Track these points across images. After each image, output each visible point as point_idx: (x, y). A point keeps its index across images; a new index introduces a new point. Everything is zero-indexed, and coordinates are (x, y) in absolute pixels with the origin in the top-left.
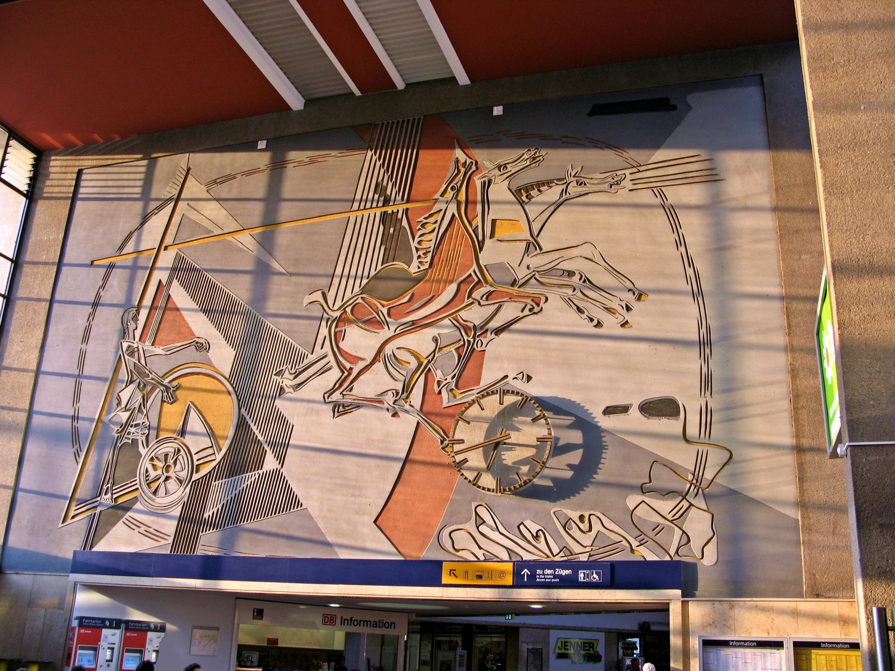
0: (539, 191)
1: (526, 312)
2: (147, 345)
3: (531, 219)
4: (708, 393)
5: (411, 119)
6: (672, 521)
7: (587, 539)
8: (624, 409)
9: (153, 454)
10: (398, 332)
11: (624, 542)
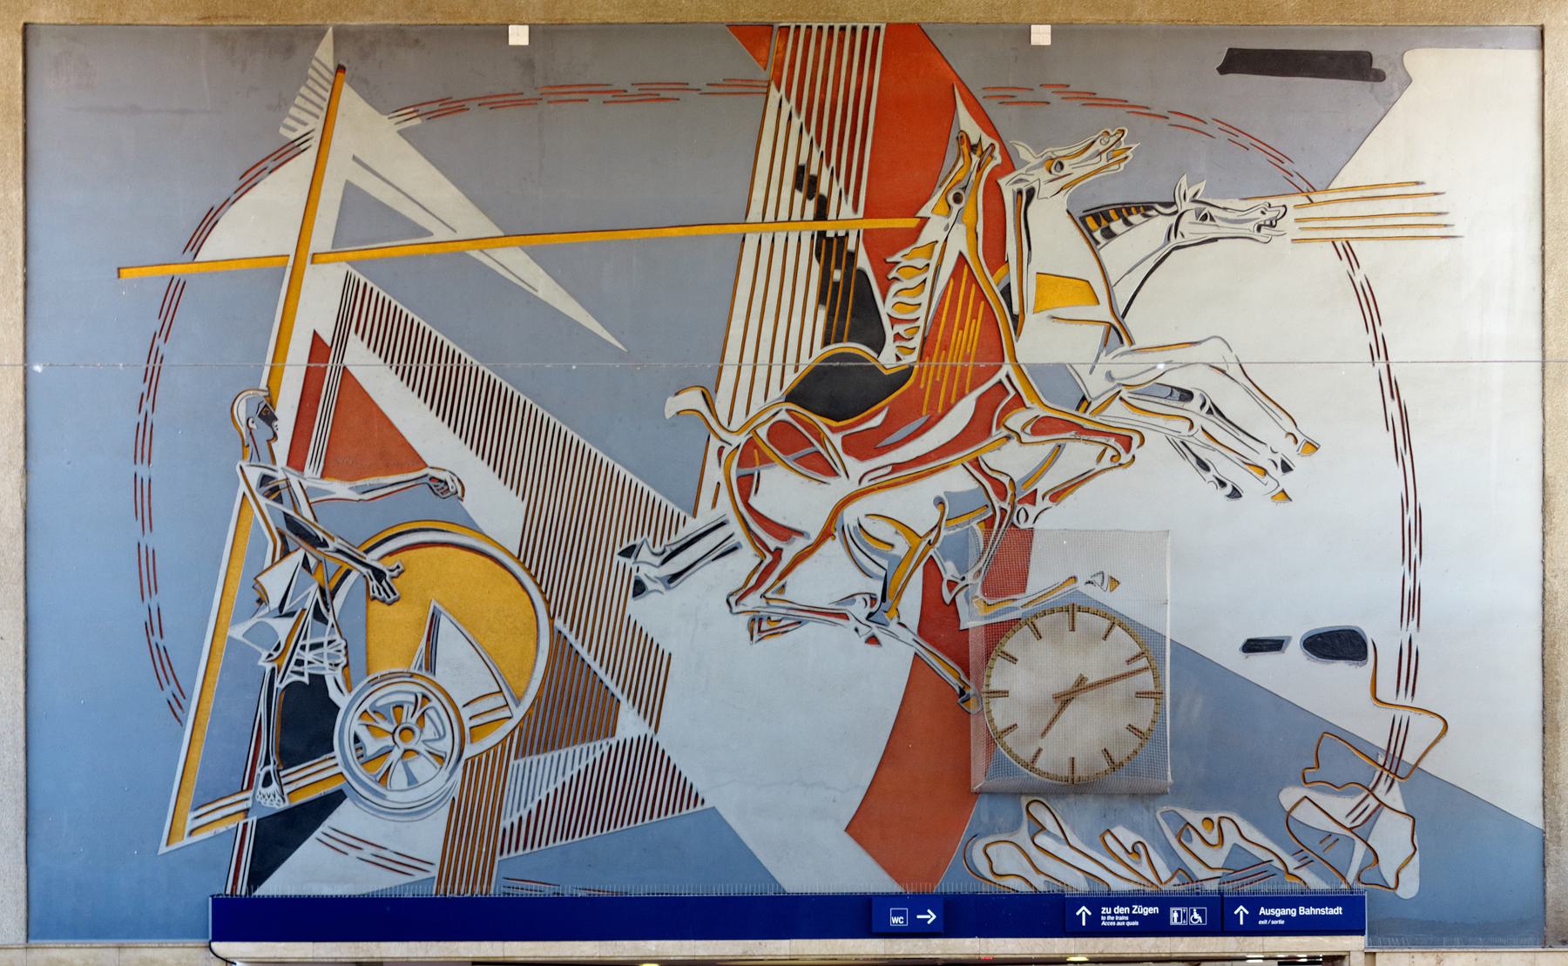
0: (1127, 223)
1: (1106, 462)
4: (1413, 624)
5: (860, 27)
6: (1350, 829)
7: (1217, 858)
8: (1276, 645)
9: (366, 706)
10: (865, 483)
11: (1277, 863)
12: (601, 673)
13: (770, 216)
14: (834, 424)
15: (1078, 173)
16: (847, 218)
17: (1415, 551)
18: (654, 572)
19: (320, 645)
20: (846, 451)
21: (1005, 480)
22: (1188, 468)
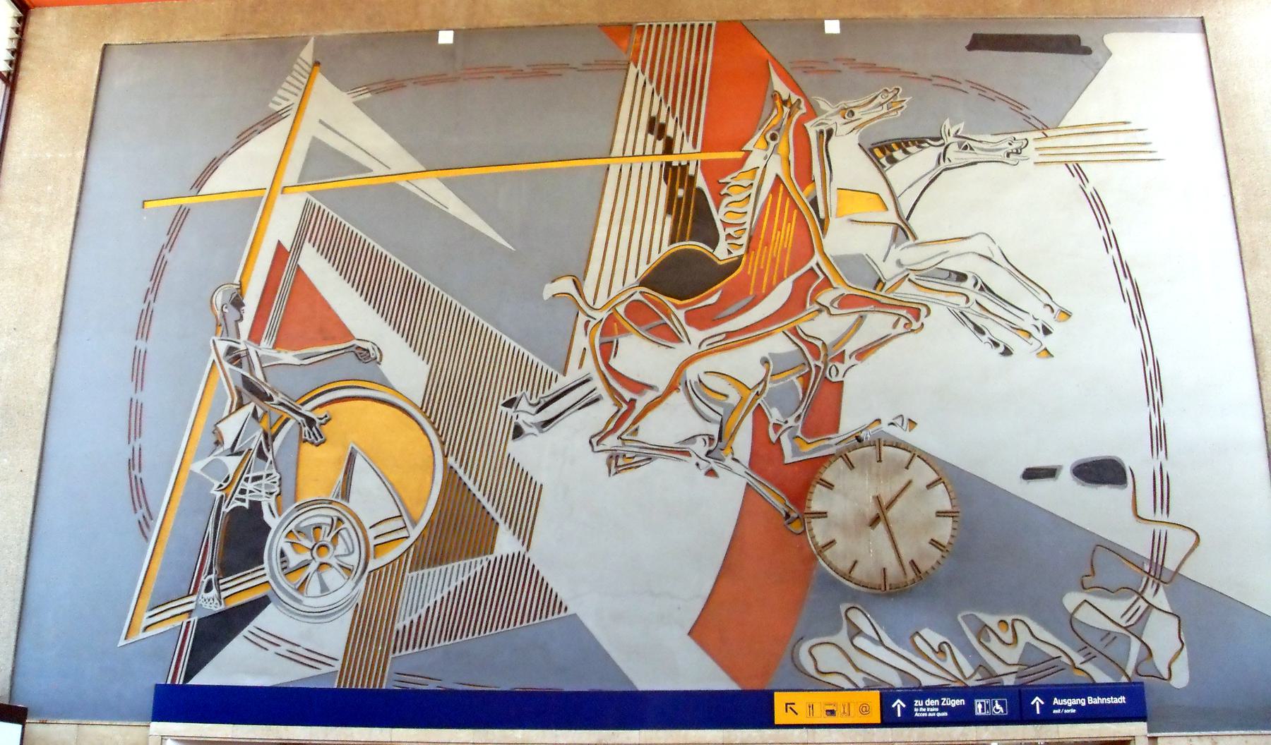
0: (905, 152)
1: (900, 329)
2: (265, 347)
3: (897, 193)
4: (1162, 453)
5: (697, 25)
6: (1125, 628)
7: (1013, 655)
8: (1051, 473)
9: (292, 527)
10: (704, 347)
12: (484, 501)
13: (629, 152)
14: (678, 302)
15: (866, 118)
16: (688, 153)
17: (1157, 395)
18: (530, 419)
19: (259, 478)
21: (819, 343)
22: (967, 333)
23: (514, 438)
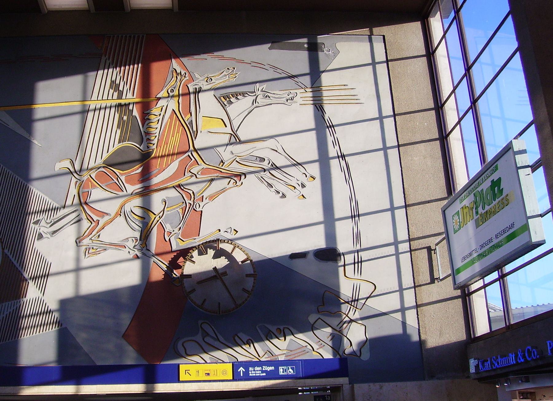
0: (237, 98)
18: (46, 230)
20: (127, 182)
22: (264, 187)
23: (38, 239)
